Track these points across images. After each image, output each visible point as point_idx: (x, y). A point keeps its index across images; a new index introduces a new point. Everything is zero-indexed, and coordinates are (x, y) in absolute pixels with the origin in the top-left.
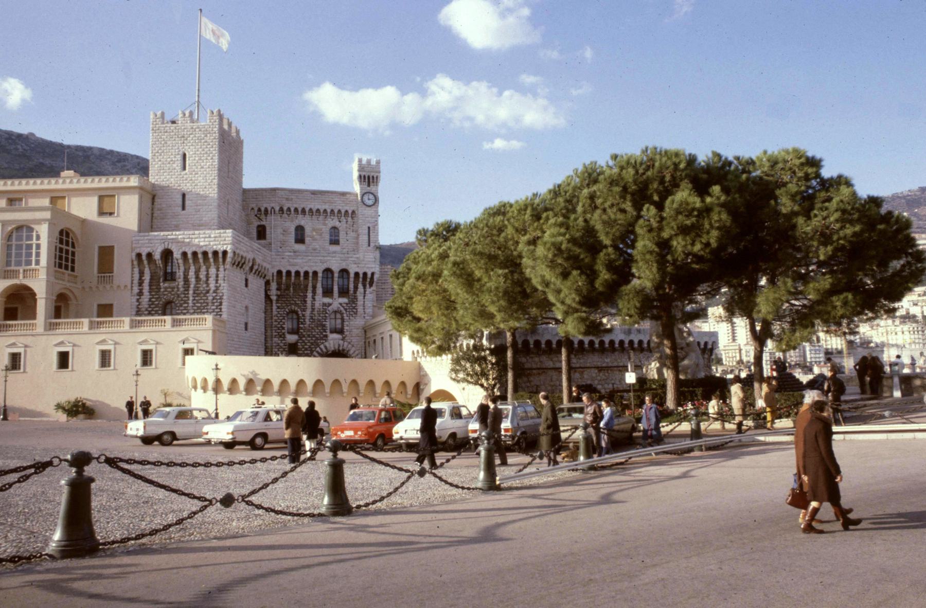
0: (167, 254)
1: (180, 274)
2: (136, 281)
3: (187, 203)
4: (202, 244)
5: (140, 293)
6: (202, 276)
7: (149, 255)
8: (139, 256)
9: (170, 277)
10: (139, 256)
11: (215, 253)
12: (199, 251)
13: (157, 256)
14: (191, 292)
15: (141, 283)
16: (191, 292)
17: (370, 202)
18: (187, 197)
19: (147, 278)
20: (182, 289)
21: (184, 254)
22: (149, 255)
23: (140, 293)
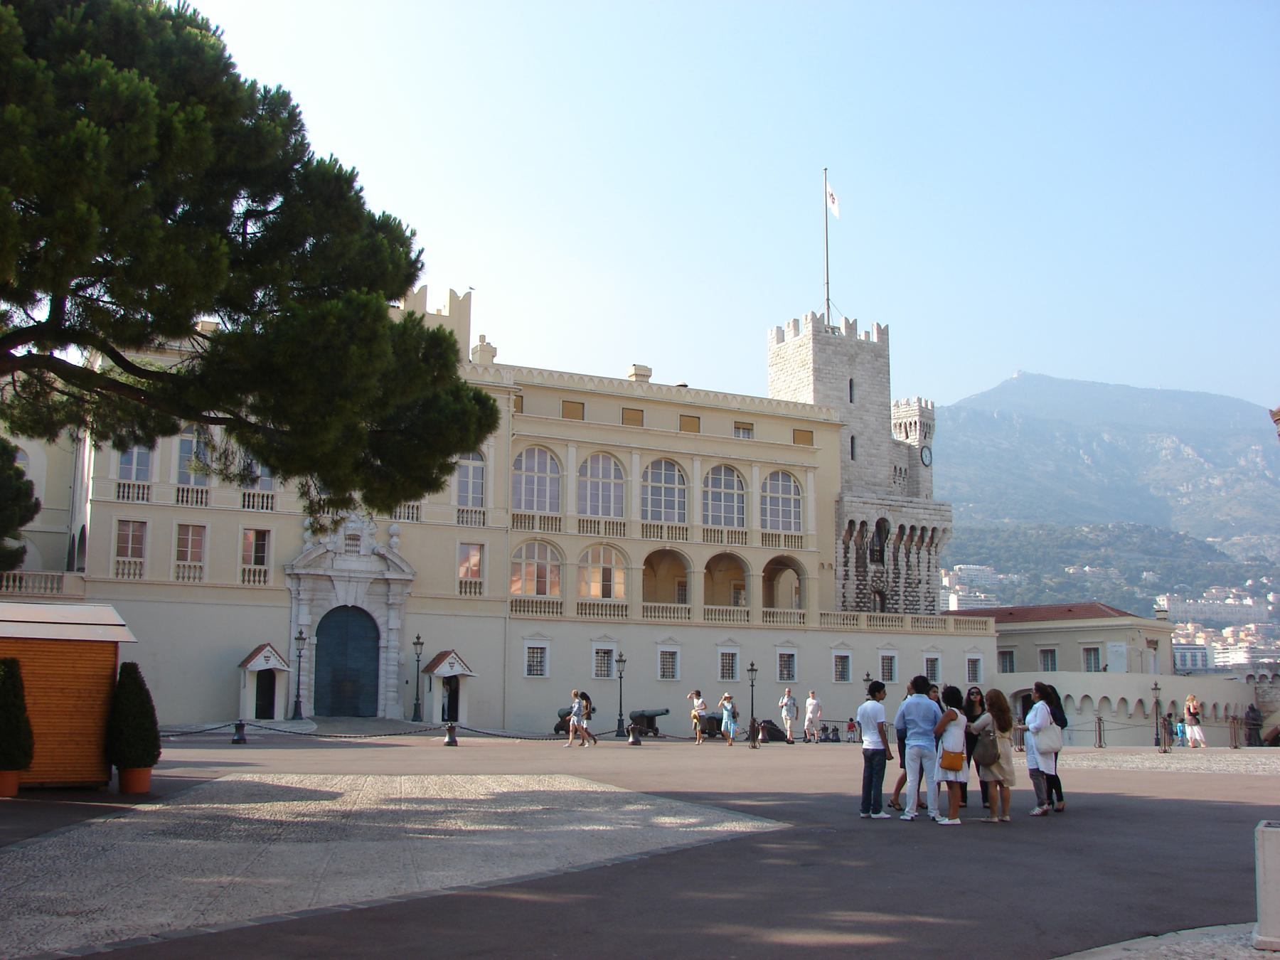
0: (882, 525)
1: (888, 554)
2: (841, 560)
3: (858, 450)
4: (921, 516)
5: (846, 576)
6: (913, 558)
7: (863, 524)
8: (852, 523)
9: (879, 558)
10: (852, 523)
11: (934, 530)
12: (919, 525)
13: (872, 528)
14: (902, 580)
15: (846, 564)
16: (902, 580)
17: (927, 462)
18: (857, 442)
19: (852, 555)
20: (891, 576)
21: (902, 528)
22: (863, 524)
23: (846, 576)
